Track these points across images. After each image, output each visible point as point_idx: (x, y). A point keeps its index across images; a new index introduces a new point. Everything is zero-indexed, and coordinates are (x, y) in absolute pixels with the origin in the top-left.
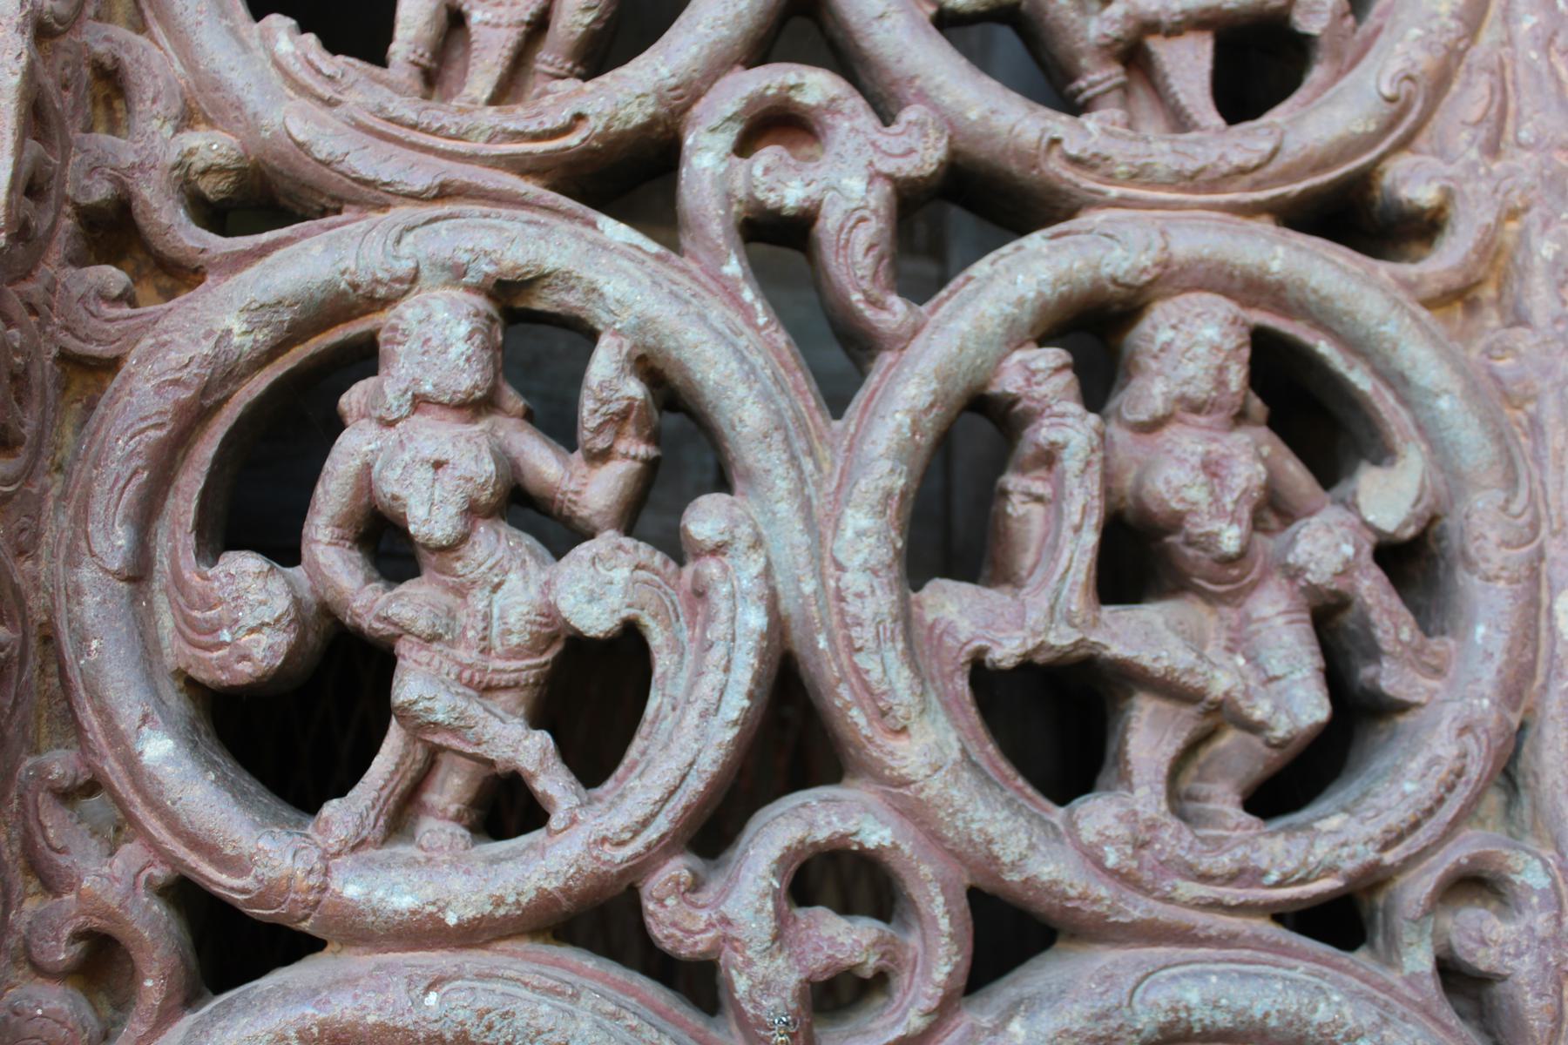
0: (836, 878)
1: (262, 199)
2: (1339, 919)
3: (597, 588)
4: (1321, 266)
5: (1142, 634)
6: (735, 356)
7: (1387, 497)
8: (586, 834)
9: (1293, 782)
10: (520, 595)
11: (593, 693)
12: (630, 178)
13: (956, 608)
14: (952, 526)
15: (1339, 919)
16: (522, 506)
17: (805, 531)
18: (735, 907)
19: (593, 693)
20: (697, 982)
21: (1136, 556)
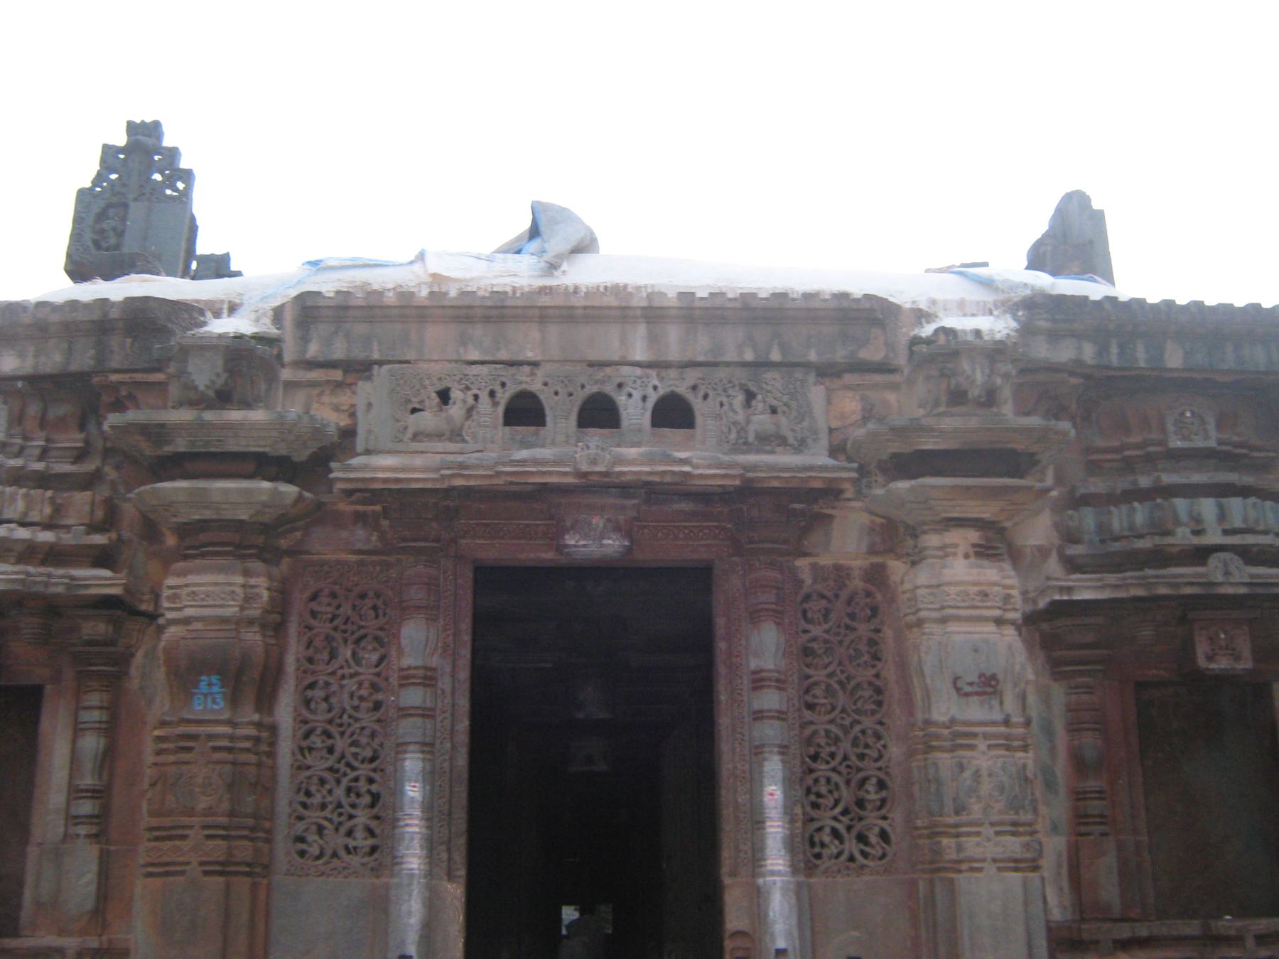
0: (848, 767)
1: (812, 723)
2: (880, 769)
3: (833, 749)
4: (878, 727)
5: (867, 751)
6: (840, 733)
7: (882, 742)
8: (833, 764)
9: (876, 760)
10: (828, 749)
11: (832, 755)
12: (832, 721)
13: (855, 750)
14: (855, 743)
15: (880, 769)
16: (828, 744)
17: (846, 746)
18: (842, 769)
19: (832, 755)
20: (839, 773)
21: (867, 746)
